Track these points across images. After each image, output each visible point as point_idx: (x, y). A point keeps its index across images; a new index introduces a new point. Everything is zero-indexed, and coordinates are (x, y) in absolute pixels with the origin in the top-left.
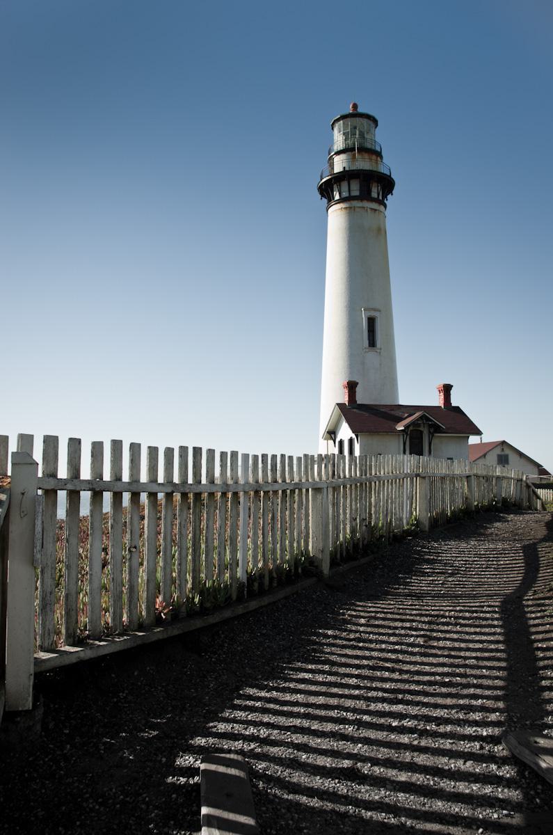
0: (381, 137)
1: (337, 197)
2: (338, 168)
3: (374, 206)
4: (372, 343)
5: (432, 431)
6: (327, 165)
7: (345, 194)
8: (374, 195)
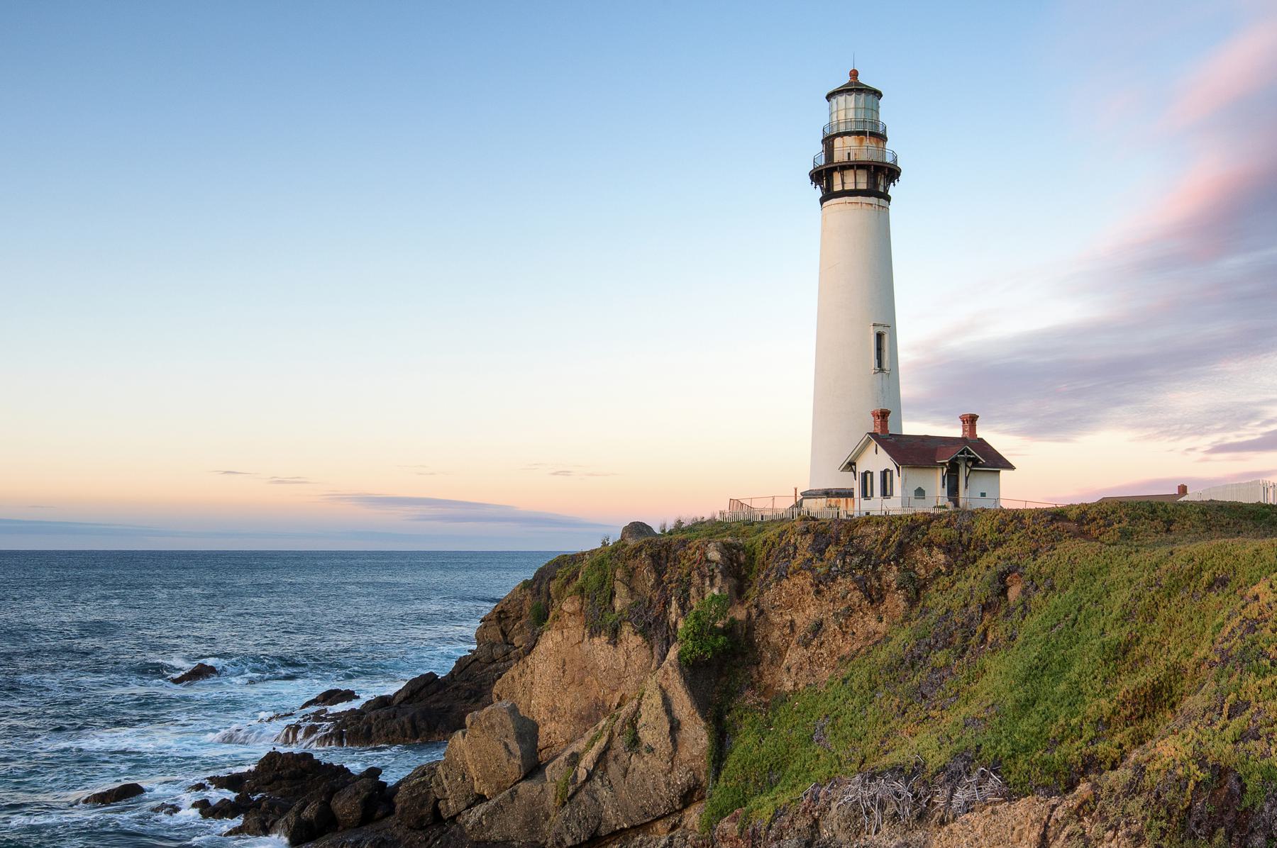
0: (888, 114)
1: (837, 187)
2: (839, 156)
3: (882, 202)
4: (880, 364)
5: (970, 464)
6: (819, 148)
7: (850, 186)
8: (881, 189)
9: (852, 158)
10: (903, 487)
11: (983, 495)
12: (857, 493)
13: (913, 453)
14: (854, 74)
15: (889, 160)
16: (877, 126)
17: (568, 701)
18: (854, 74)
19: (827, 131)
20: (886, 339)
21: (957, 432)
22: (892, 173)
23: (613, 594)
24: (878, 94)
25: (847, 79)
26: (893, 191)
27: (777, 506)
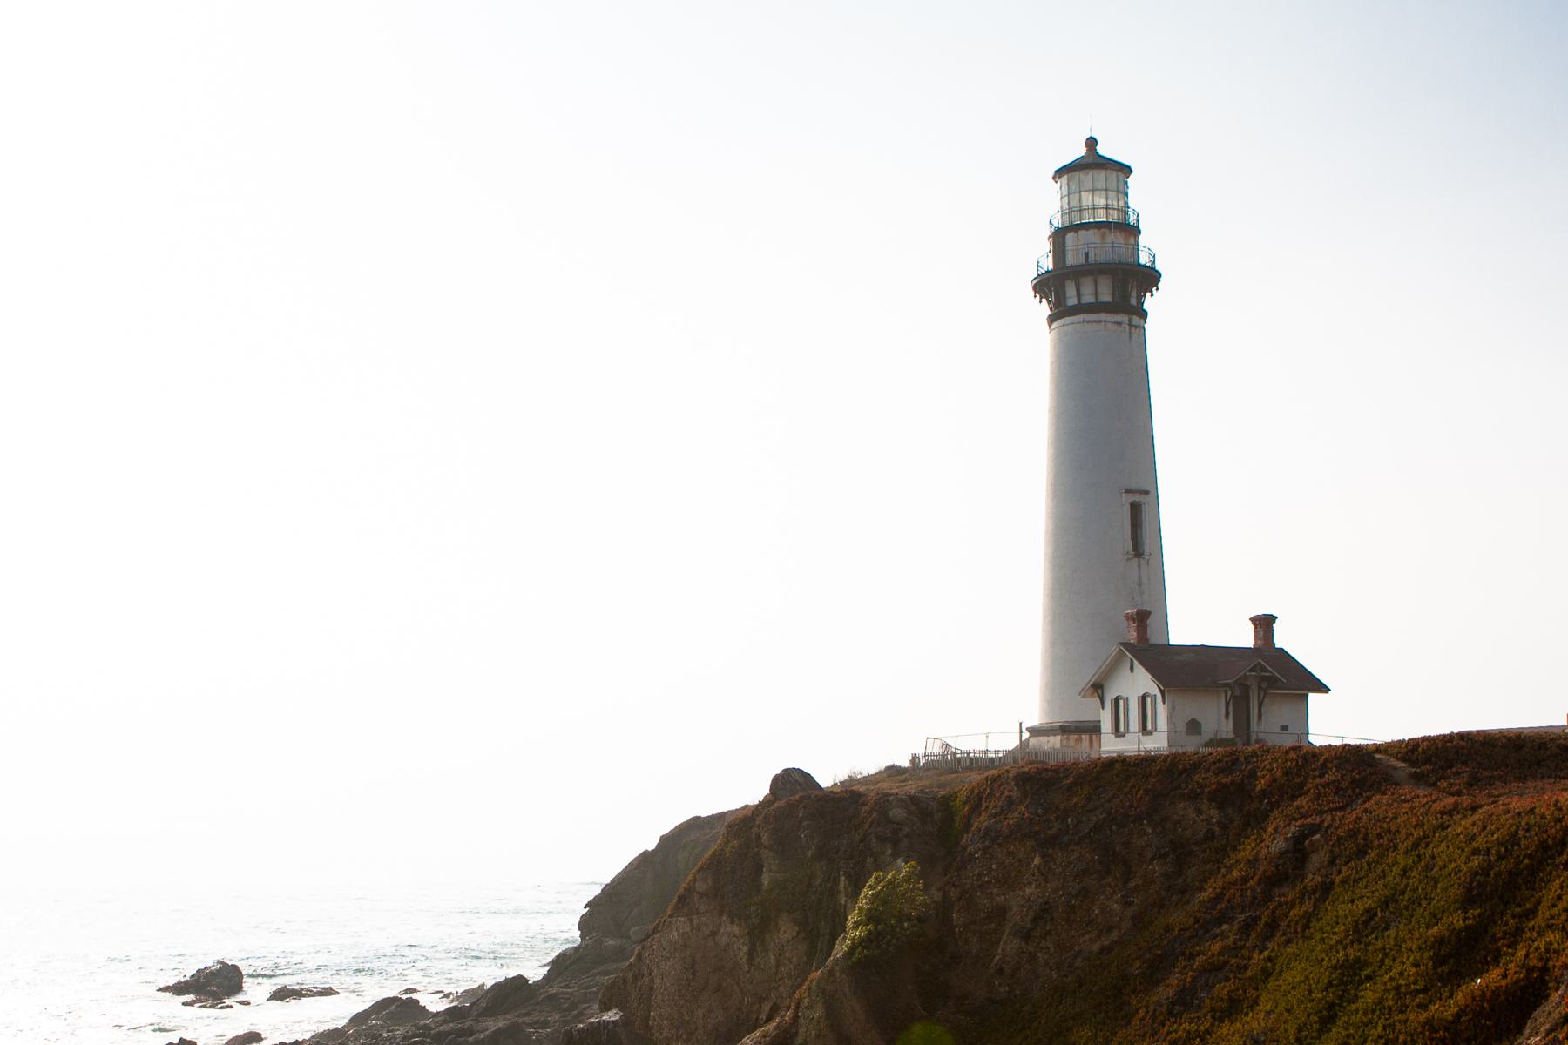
0: (1141, 199)
3: (1136, 320)
6: (1047, 246)
7: (1088, 298)
8: (1134, 301)
9: (1092, 259)
10: (1170, 718)
11: (1284, 728)
12: (1106, 725)
13: (1189, 671)
14: (1091, 143)
15: (1144, 259)
16: (1126, 213)
17: (700, 1012)
18: (1091, 143)
19: (1057, 223)
20: (1146, 509)
21: (1245, 638)
22: (1149, 278)
23: (758, 869)
24: (1126, 170)
25: (1082, 151)
26: (1149, 303)
27: (992, 748)
